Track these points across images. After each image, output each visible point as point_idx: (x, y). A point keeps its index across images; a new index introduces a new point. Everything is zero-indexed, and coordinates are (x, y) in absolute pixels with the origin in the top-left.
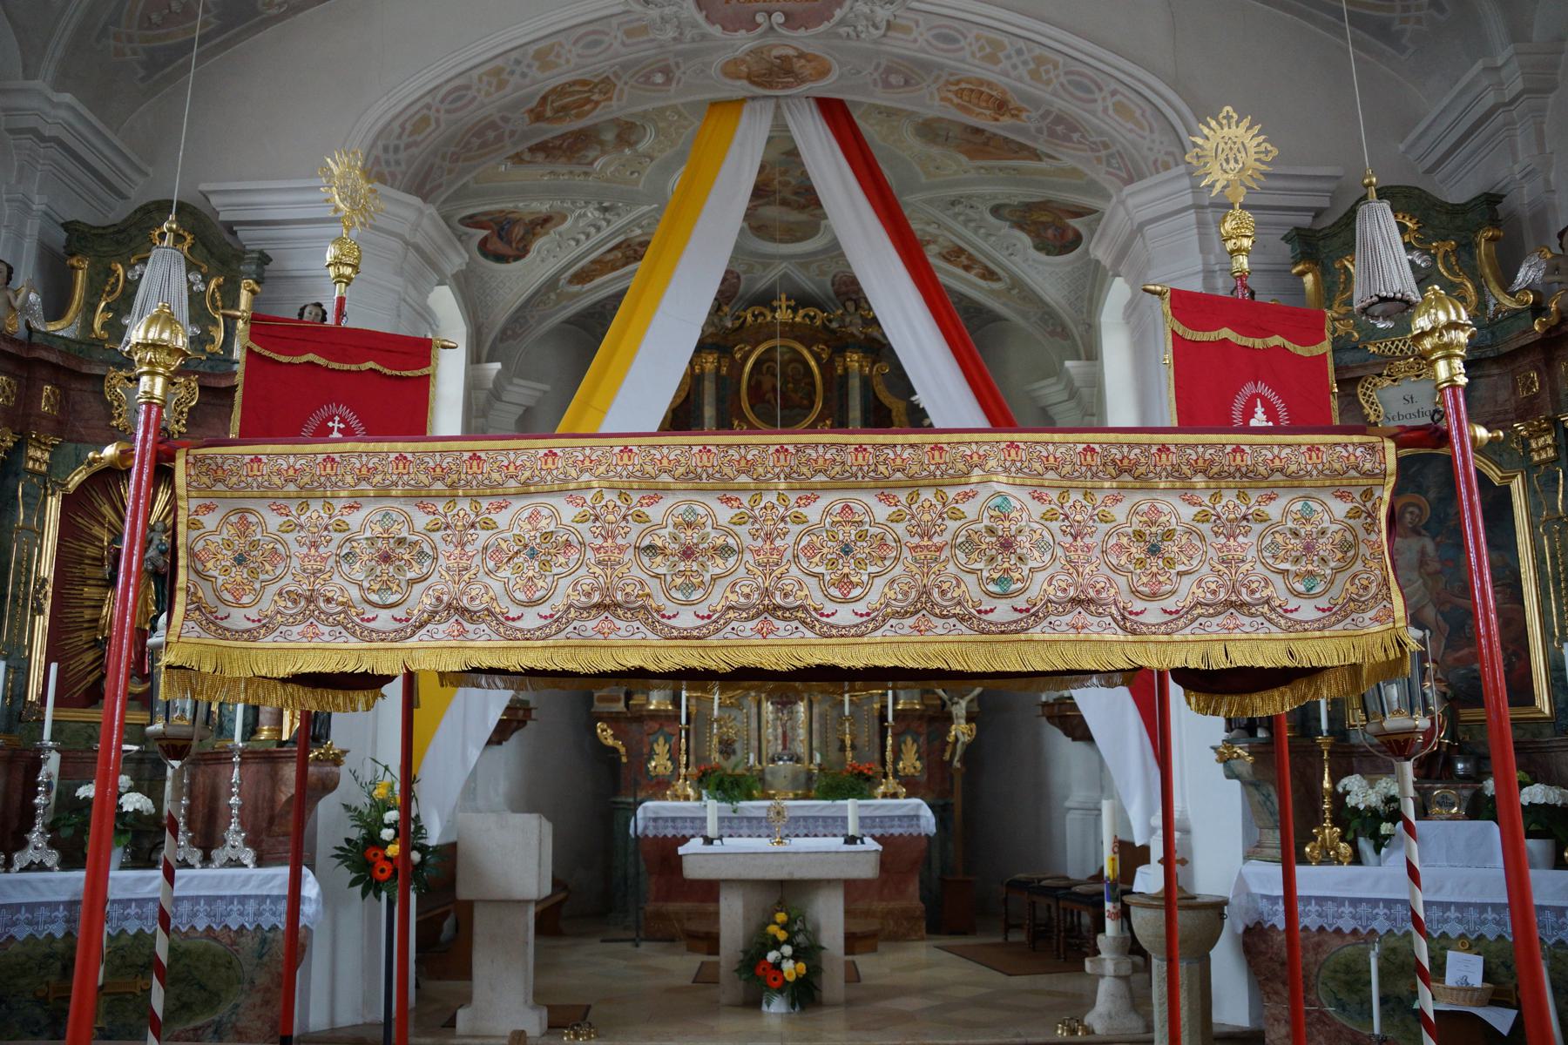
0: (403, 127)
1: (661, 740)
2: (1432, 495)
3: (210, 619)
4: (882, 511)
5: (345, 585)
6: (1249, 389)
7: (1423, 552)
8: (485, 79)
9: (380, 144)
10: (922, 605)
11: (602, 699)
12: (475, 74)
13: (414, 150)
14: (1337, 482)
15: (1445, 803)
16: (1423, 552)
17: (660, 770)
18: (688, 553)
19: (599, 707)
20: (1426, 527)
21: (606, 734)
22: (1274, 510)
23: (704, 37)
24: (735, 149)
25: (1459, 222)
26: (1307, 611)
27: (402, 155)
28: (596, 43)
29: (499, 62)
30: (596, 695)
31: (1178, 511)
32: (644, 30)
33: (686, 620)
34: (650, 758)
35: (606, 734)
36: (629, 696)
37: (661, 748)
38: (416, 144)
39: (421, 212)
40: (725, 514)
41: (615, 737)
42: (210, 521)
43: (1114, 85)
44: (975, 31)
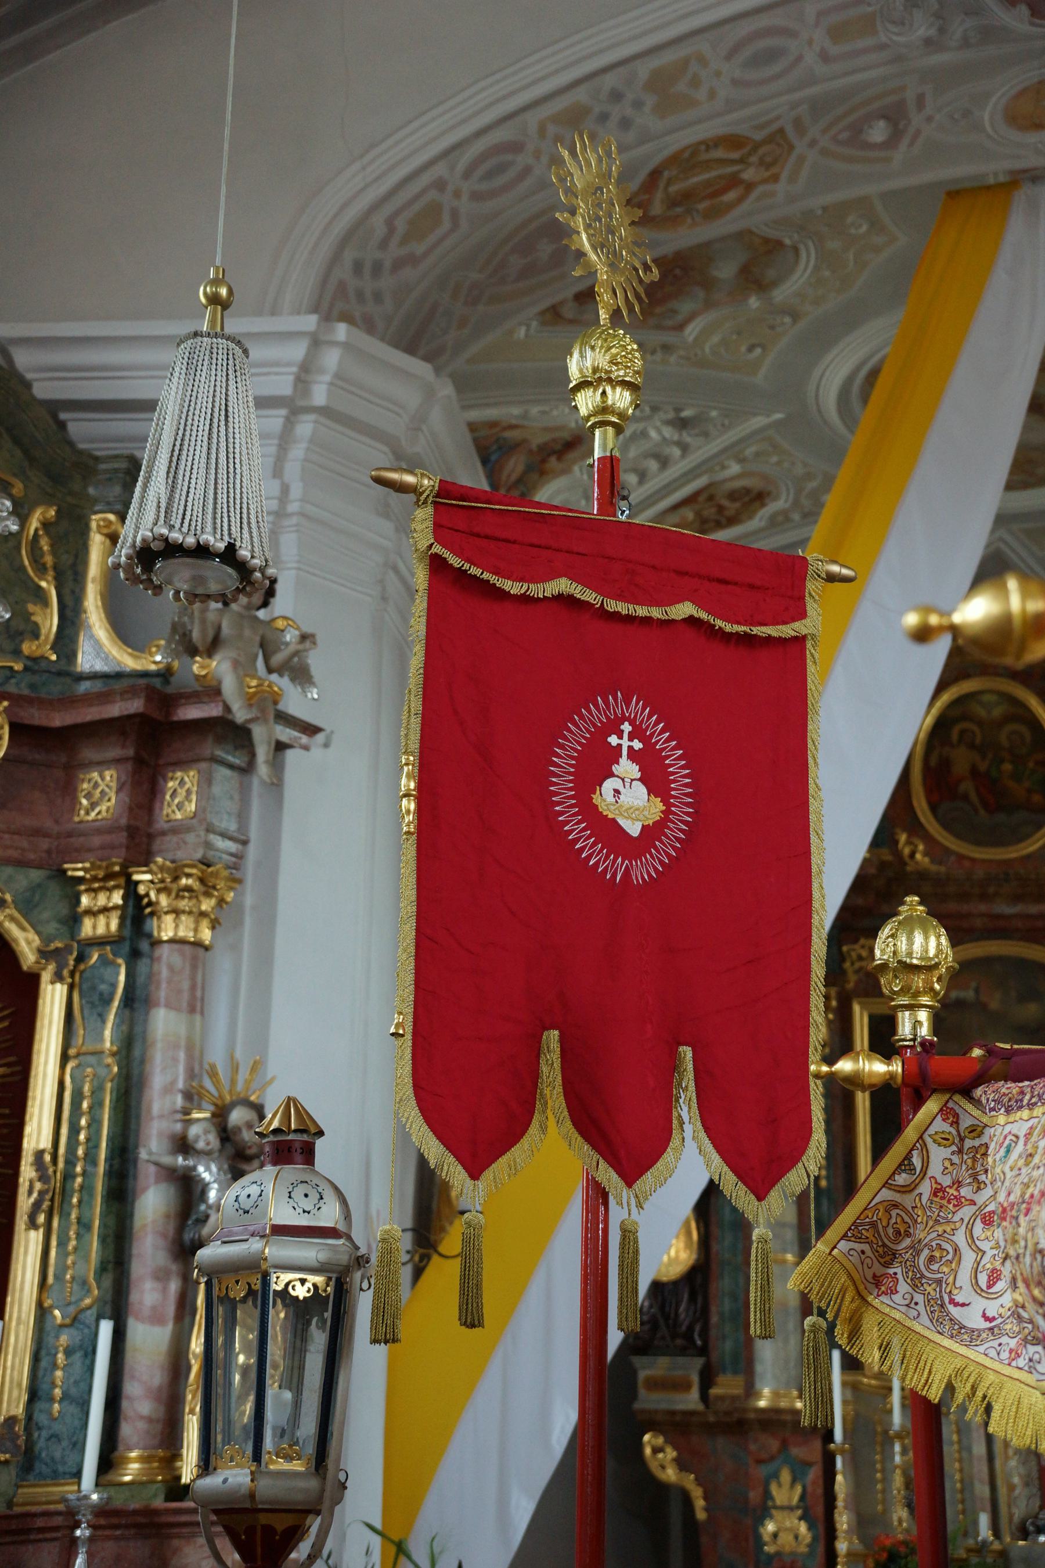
0: (390, 222)
1: (786, 1476)
8: (552, 129)
9: (349, 256)
11: (654, 1384)
12: (532, 119)
13: (409, 273)
17: (786, 1540)
19: (648, 1400)
28: (771, 56)
29: (580, 95)
30: (642, 1375)
36: (707, 1380)
37: (785, 1492)
38: (412, 260)
39: (429, 394)
41: (681, 1464)
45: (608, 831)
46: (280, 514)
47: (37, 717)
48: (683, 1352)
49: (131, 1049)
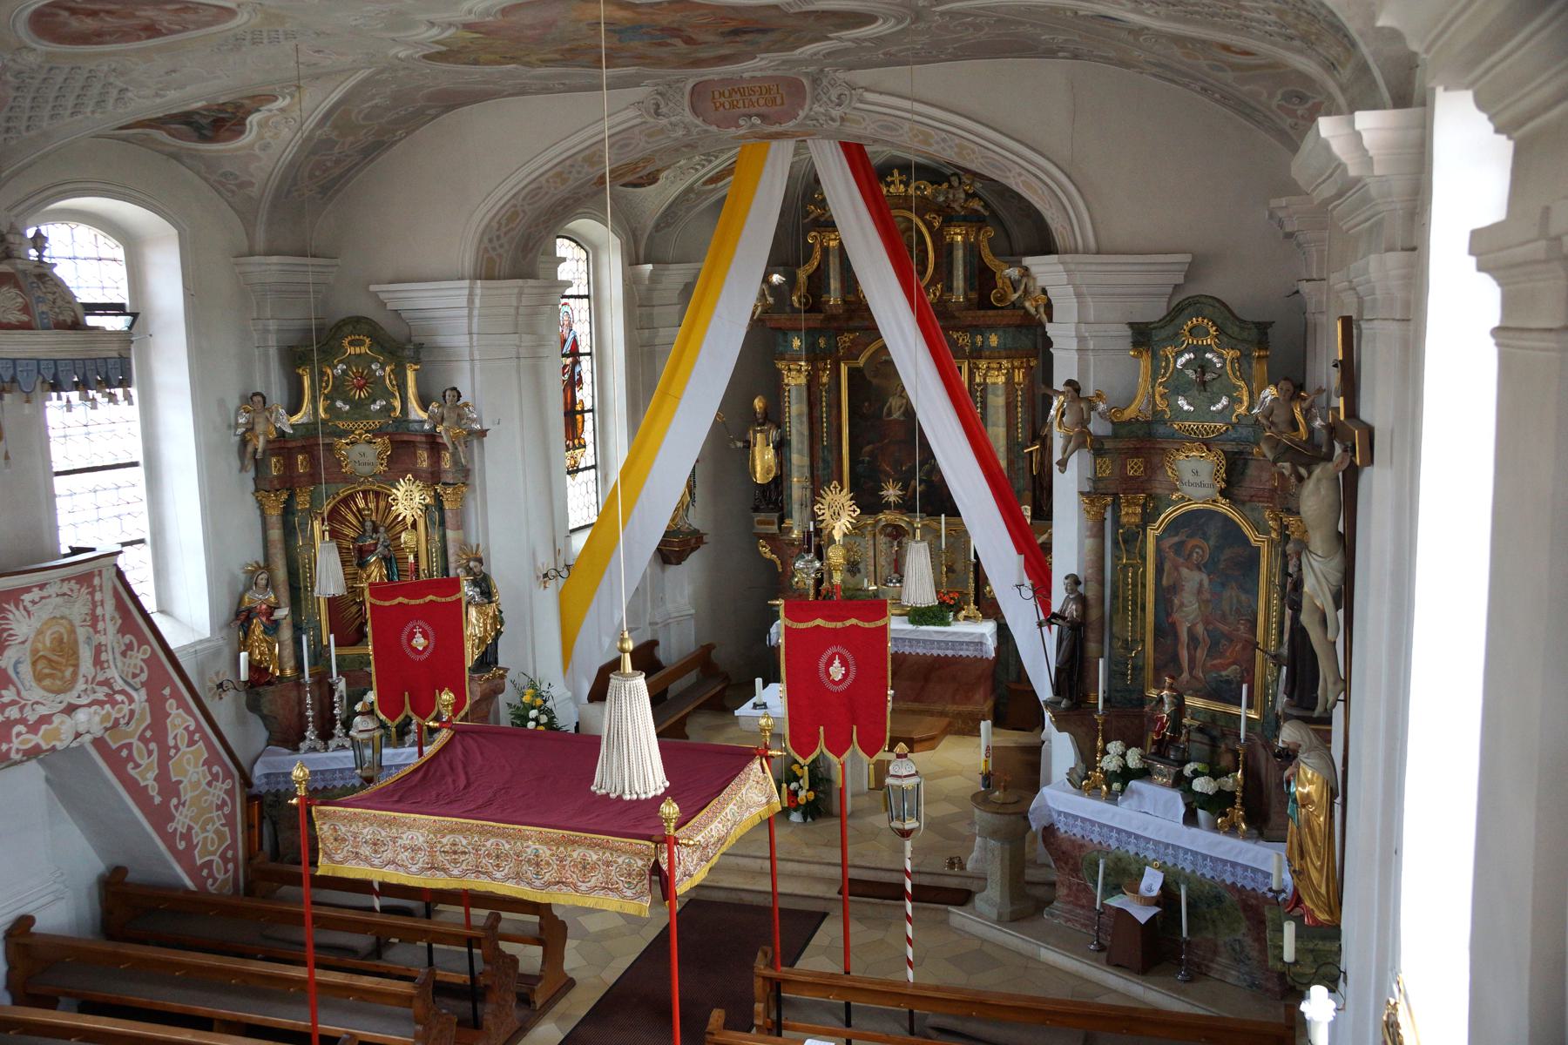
0: (499, 223)
2: (1212, 543)
3: (328, 855)
4: (507, 846)
5: (366, 851)
6: (829, 652)
7: (1201, 584)
9: (486, 240)
10: (518, 877)
11: (760, 523)
14: (638, 854)
15: (1160, 773)
16: (1201, 584)
18: (455, 853)
20: (1205, 566)
21: (766, 551)
22: (620, 860)
23: (706, 131)
24: (768, 168)
25: (1245, 335)
26: (629, 893)
27: (504, 240)
28: (627, 145)
29: (558, 169)
31: (593, 856)
32: (662, 131)
33: (456, 872)
34: (794, 575)
35: (766, 551)
36: (781, 521)
40: (464, 842)
42: (325, 827)
43: (1018, 170)
44: (907, 125)
45: (415, 650)
46: (471, 346)
47: (398, 438)
48: (772, 510)
49: (444, 538)
